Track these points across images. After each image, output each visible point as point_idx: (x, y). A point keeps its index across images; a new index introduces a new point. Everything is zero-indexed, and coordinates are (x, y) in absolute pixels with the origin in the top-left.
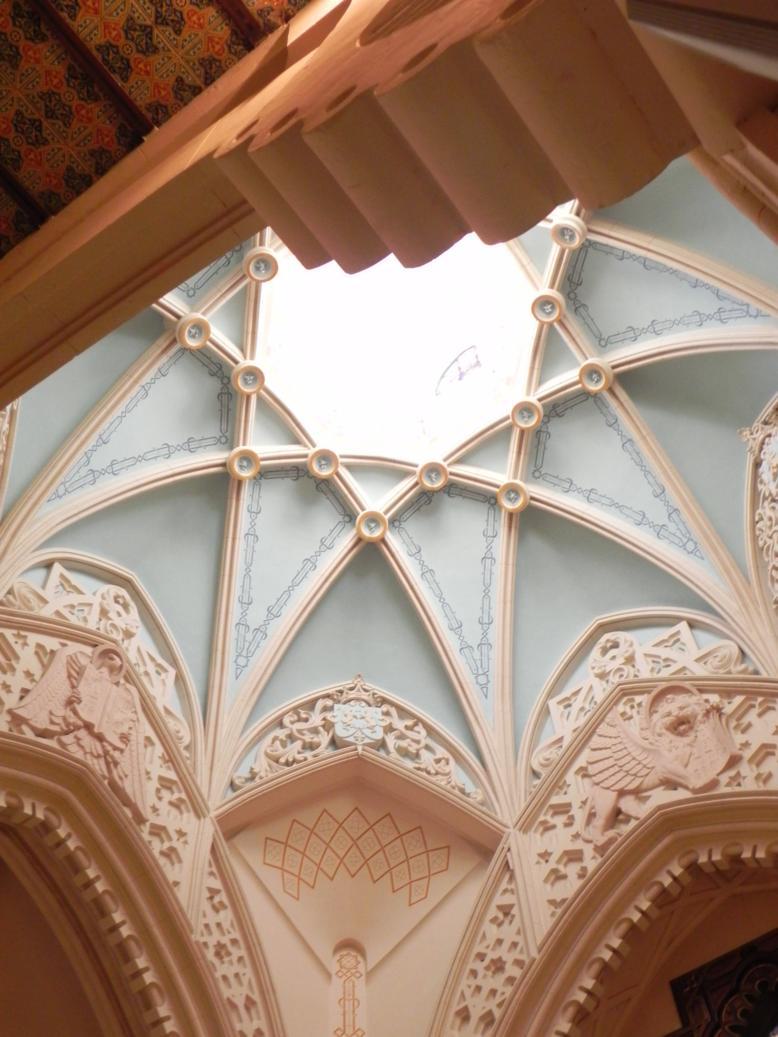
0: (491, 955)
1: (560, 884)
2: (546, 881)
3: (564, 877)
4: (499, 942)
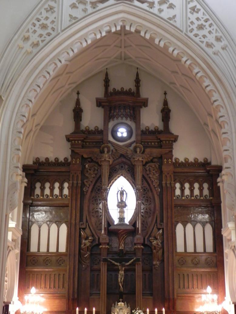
0: (43, 21)
1: (75, 10)
2: (70, 6)
3: (77, 8)
4: (47, 18)
